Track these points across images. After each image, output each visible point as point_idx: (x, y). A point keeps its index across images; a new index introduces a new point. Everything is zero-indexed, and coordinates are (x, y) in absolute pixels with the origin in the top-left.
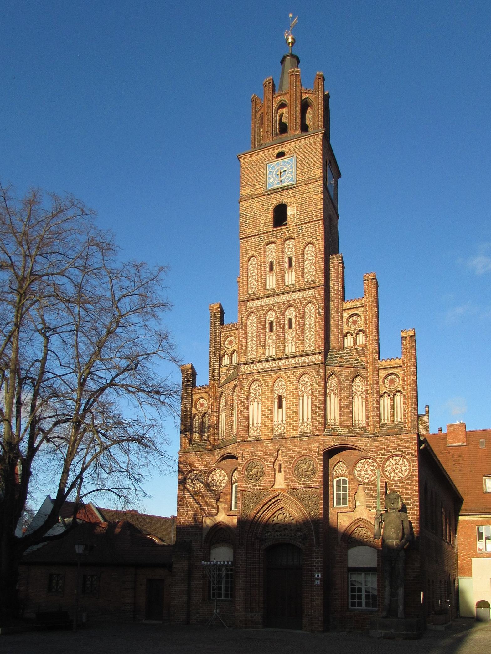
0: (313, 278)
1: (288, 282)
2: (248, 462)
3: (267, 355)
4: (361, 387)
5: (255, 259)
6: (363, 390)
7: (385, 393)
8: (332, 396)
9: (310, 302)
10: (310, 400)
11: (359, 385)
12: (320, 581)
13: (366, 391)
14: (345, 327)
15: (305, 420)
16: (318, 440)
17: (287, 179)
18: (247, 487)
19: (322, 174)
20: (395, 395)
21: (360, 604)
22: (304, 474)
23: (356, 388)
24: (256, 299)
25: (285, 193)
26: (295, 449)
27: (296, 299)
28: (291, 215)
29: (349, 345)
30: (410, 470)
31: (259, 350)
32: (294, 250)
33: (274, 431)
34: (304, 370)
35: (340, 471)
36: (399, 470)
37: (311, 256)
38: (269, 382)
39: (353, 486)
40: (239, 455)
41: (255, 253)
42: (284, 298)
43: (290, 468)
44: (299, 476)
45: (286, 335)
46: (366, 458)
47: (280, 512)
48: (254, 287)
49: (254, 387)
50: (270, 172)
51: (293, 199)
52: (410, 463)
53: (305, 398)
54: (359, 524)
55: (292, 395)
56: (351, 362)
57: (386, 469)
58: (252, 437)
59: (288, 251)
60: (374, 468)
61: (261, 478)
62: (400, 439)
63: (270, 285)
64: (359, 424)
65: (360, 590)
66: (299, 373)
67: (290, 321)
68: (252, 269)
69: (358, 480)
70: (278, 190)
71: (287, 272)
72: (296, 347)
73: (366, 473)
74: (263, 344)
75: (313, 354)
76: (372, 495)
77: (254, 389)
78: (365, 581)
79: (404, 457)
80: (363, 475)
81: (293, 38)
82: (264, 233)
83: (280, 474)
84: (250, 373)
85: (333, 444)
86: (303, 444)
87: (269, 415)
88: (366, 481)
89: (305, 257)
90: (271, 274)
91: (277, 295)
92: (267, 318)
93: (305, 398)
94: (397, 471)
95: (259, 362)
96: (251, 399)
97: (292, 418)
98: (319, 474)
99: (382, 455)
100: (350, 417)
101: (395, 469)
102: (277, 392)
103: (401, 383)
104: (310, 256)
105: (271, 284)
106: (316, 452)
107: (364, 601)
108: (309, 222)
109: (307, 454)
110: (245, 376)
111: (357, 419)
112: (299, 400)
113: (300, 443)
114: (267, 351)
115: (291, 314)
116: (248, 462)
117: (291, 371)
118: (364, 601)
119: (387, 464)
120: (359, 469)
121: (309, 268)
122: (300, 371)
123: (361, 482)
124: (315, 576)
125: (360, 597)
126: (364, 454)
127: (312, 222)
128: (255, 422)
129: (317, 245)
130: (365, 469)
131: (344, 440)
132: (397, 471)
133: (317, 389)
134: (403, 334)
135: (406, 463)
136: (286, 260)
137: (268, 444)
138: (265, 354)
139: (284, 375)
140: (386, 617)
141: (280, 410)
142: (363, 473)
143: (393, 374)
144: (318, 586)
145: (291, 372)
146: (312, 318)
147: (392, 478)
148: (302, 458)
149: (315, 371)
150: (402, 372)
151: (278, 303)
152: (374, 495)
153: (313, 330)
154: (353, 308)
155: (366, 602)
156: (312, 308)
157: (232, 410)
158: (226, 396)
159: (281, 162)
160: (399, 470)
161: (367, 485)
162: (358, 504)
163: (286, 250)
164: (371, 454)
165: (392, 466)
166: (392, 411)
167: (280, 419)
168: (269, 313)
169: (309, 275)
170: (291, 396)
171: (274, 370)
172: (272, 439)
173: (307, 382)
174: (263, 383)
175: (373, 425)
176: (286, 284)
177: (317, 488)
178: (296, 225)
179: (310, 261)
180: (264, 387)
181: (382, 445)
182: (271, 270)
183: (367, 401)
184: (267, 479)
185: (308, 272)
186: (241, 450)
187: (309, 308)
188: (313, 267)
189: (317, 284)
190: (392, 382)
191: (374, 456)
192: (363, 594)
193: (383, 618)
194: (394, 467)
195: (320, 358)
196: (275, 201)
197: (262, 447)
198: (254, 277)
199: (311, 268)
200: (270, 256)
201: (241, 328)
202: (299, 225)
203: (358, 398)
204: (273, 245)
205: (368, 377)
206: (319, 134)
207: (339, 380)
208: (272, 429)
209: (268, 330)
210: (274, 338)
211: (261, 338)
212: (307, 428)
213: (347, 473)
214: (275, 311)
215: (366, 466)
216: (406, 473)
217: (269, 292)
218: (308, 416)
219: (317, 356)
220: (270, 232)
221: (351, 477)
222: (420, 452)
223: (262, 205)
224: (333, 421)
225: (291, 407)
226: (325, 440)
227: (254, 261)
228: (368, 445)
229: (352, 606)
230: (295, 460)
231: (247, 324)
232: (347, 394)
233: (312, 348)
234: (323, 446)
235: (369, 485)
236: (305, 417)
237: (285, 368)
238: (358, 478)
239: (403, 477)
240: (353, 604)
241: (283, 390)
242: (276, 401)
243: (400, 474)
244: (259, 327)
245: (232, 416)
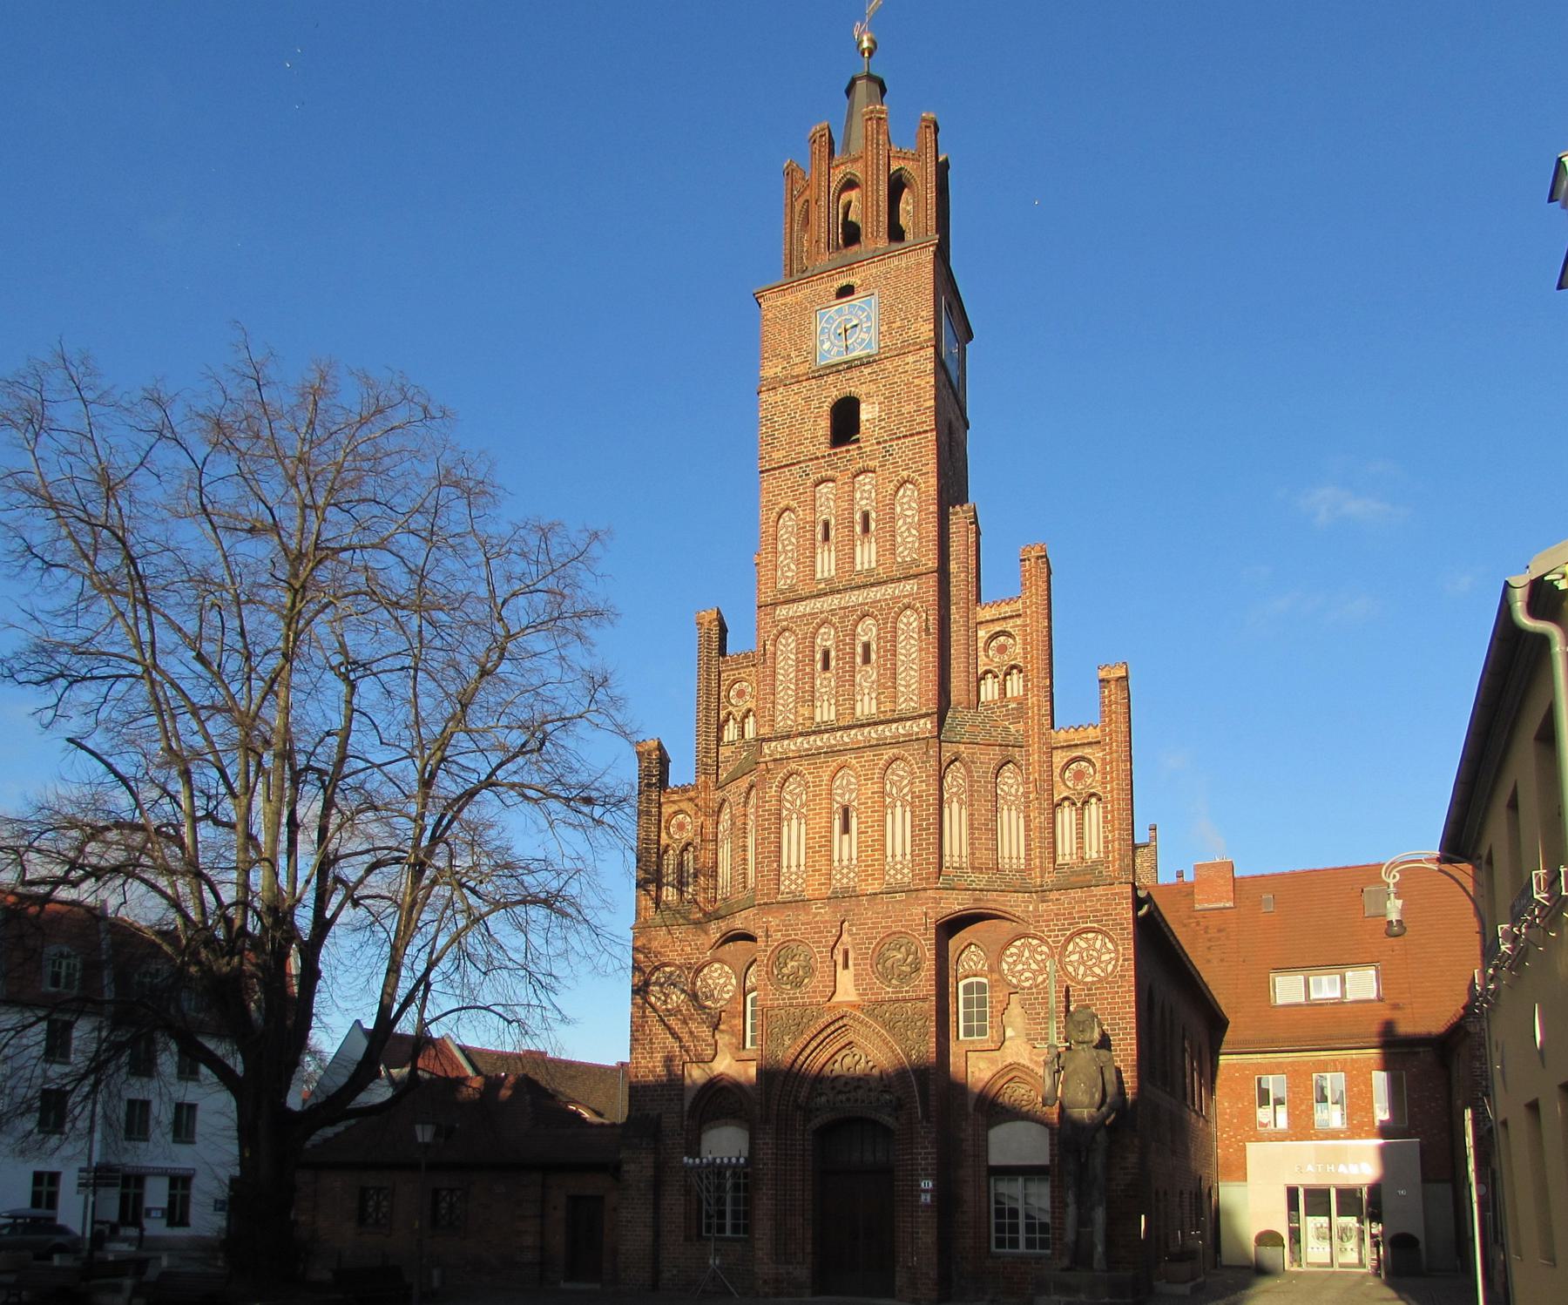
0: (914, 556)
1: (862, 564)
2: (780, 948)
3: (818, 719)
4: (1015, 787)
5: (793, 516)
6: (1019, 794)
7: (1066, 798)
8: (955, 806)
9: (907, 607)
10: (908, 815)
11: (1010, 783)
12: (932, 1196)
13: (1026, 794)
14: (982, 659)
15: (899, 858)
16: (926, 899)
17: (860, 344)
18: (778, 999)
19: (932, 334)
20: (1085, 802)
21: (1014, 1243)
22: (896, 972)
23: (1005, 788)
24: (794, 601)
25: (855, 373)
26: (876, 918)
27: (879, 601)
28: (867, 421)
29: (990, 698)
30: (1117, 960)
31: (801, 710)
32: (873, 495)
33: (834, 882)
34: (895, 751)
35: (972, 964)
36: (1094, 961)
37: (910, 508)
38: (821, 776)
39: (999, 997)
40: (759, 933)
41: (792, 502)
42: (855, 598)
43: (867, 959)
44: (885, 977)
45: (858, 677)
46: (1026, 936)
47: (848, 1052)
48: (790, 574)
49: (791, 788)
50: (823, 328)
51: (873, 387)
52: (1117, 945)
53: (899, 811)
54: (1011, 1075)
55: (870, 804)
56: (994, 734)
57: (1067, 960)
58: (787, 893)
59: (862, 499)
60: (1044, 957)
61: (806, 981)
62: (1096, 896)
63: (823, 572)
64: (1011, 866)
65: (1014, 1213)
66: (886, 757)
67: (867, 647)
68: (785, 537)
69: (1009, 984)
70: (841, 368)
71: (859, 543)
72: (879, 704)
73: (1025, 967)
74: (809, 697)
75: (914, 718)
76: (1039, 1014)
77: (791, 792)
78: (1026, 1196)
79: (1106, 934)
80: (1019, 972)
81: (872, 41)
82: (811, 460)
83: (846, 972)
84: (782, 759)
85: (958, 908)
86: (893, 907)
87: (822, 847)
88: (1027, 984)
89: (898, 509)
90: (826, 548)
91: (839, 592)
92: (819, 641)
93: (899, 811)
94: (1090, 963)
95: (801, 734)
96: (785, 813)
97: (870, 853)
98: (928, 970)
100: (992, 850)
101: (1085, 958)
102: (838, 798)
103: (1098, 777)
104: (907, 509)
105: (826, 568)
106: (921, 925)
107: (1022, 1236)
108: (905, 437)
110: (771, 765)
111: (1006, 855)
112: (884, 816)
113: (888, 907)
114: (818, 711)
115: (868, 631)
116: (780, 948)
117: (869, 754)
118: (1022, 1236)
119: (1071, 947)
120: (1010, 960)
121: (906, 534)
122: (889, 753)
123: (1015, 987)
124: (920, 1185)
125: (1014, 1228)
126: (1021, 929)
127: (912, 435)
128: (794, 863)
129: (923, 485)
131: (980, 900)
132: (1090, 963)
133: (923, 791)
134: (1102, 674)
135: (1110, 946)
136: (858, 517)
137: (820, 908)
138: (813, 719)
139: (854, 761)
140: (1068, 1269)
141: (846, 837)
142: (1020, 967)
143: (1082, 759)
144: (927, 1205)
146: (912, 642)
147: (1080, 977)
148: (894, 938)
150: (1101, 754)
151: (840, 609)
152: (1042, 1015)
153: (914, 667)
154: (998, 619)
155: (1027, 1239)
156: (912, 619)
157: (745, 837)
158: (731, 808)
159: (846, 306)
160: (1094, 961)
161: (1027, 994)
162: (1009, 1033)
163: (858, 495)
164: (1035, 927)
166: (1080, 836)
167: (845, 856)
168: (823, 630)
169: (906, 549)
170: (869, 807)
171: (832, 752)
172: (829, 898)
173: (903, 778)
174: (811, 780)
175: (1041, 867)
176: (858, 568)
177: (924, 999)
178: (878, 443)
179: (909, 520)
180: (812, 789)
182: (826, 538)
183: (1027, 817)
184: (819, 982)
185: (904, 542)
186: (764, 923)
187: (905, 620)
188: (914, 532)
189: (923, 569)
190: (1079, 775)
192: (1022, 1221)
193: (1063, 1270)
194: (1085, 955)
195: (929, 726)
197: (808, 914)
198: (790, 555)
200: (823, 508)
201: (762, 664)
202: (885, 441)
203: (1009, 810)
204: (831, 485)
205: (1030, 765)
206: (926, 247)
207: (969, 771)
208: (829, 876)
209: (819, 666)
210: (833, 683)
211: (806, 683)
212: (902, 874)
213: (986, 968)
214: (833, 625)
216: (1110, 968)
217: (822, 586)
219: (922, 721)
220: (824, 457)
221: (996, 976)
222: (1139, 923)
223: (807, 400)
224: (958, 859)
225: (870, 830)
226: (941, 898)
227: (790, 519)
228: (1031, 908)
229: (997, 1247)
230: (878, 943)
231: (775, 654)
232: (985, 801)
233: (913, 704)
234: (937, 913)
235: (1033, 994)
236: (899, 852)
237: (855, 746)
238: (1010, 978)
239: (1102, 974)
240: (1000, 1243)
241: (851, 794)
242: (837, 817)
243: (1097, 970)
244: (801, 662)
245: (744, 850)
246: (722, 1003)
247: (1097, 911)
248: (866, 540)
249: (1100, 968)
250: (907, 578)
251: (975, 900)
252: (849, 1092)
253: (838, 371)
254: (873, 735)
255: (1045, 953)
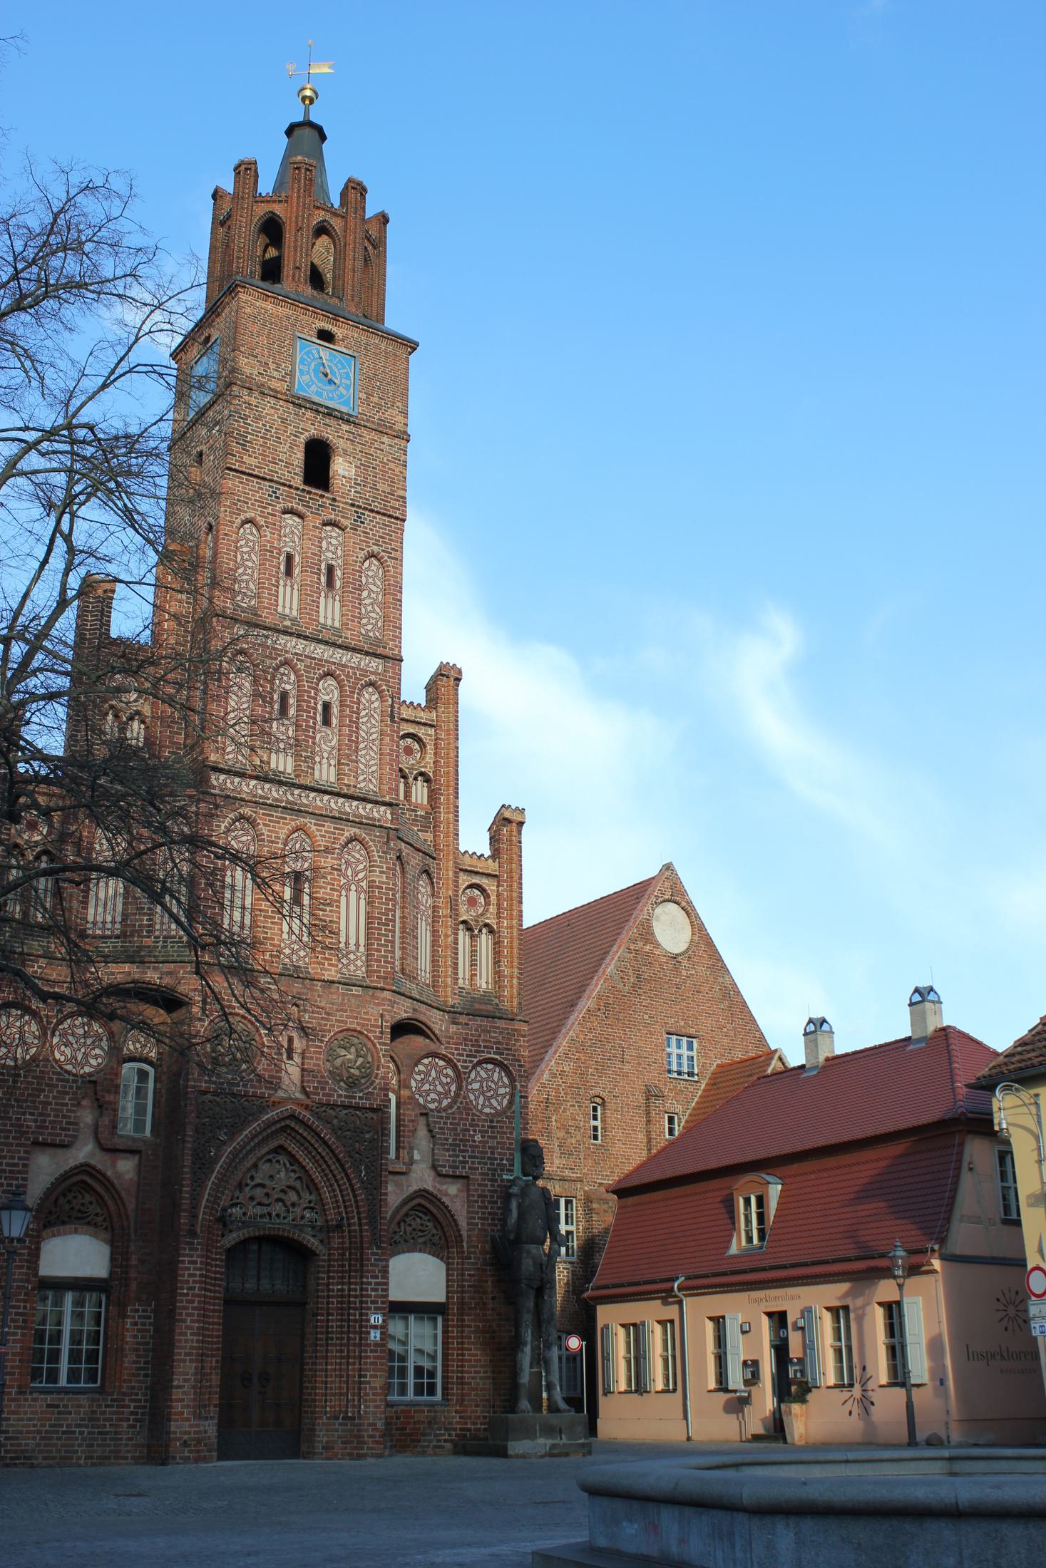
1: (326, 618)
10: (362, 903)
15: (352, 947)
16: (383, 999)
22: (345, 1075)
25: (332, 422)
32: (339, 552)
34: (357, 831)
37: (375, 584)
39: (411, 1115)
41: (258, 518)
42: (319, 651)
50: (302, 358)
51: (350, 449)
52: (515, 1081)
53: (353, 895)
60: (449, 1080)
62: (498, 1028)
66: (347, 834)
71: (323, 594)
75: (376, 803)
76: (447, 1139)
82: (284, 485)
85: (404, 1015)
86: (349, 1001)
88: (432, 1106)
90: (289, 583)
91: (306, 638)
93: (353, 895)
94: (489, 1094)
99: (467, 1056)
106: (376, 1026)
108: (378, 513)
109: (359, 1028)
110: (219, 801)
113: (343, 999)
117: (329, 826)
120: (418, 1078)
122: (350, 831)
126: (433, 1047)
127: (384, 515)
130: (431, 1079)
132: (489, 1094)
133: (383, 883)
138: (269, 763)
139: (314, 828)
142: (426, 1087)
145: (328, 827)
149: (379, 842)
151: (306, 656)
156: (374, 698)
161: (438, 1117)
162: (417, 1156)
164: (446, 1048)
165: (496, 1084)
168: (282, 670)
174: (266, 833)
178: (353, 505)
179: (373, 596)
181: (467, 1034)
182: (289, 573)
191: (453, 1054)
194: (484, 1084)
196: (313, 428)
198: (249, 571)
199: (374, 611)
202: (359, 507)
212: (356, 966)
215: (433, 1074)
216: (505, 1102)
217: (288, 623)
218: (357, 941)
219: (383, 808)
220: (297, 489)
223: (284, 420)
226: (395, 1002)
227: (252, 534)
235: (442, 1117)
239: (480, 1107)
243: (494, 1102)
246: (87, 1069)
247: (498, 1043)
248: (330, 595)
249: (497, 1100)
250: (375, 655)
251: (415, 1010)
252: (269, 1205)
253: (317, 411)
254: (333, 805)
255: (450, 1076)
